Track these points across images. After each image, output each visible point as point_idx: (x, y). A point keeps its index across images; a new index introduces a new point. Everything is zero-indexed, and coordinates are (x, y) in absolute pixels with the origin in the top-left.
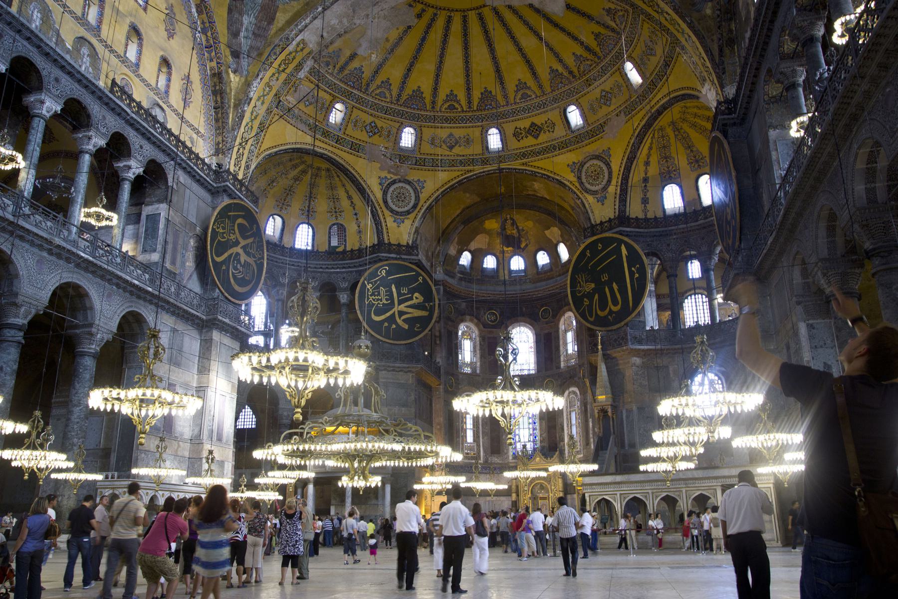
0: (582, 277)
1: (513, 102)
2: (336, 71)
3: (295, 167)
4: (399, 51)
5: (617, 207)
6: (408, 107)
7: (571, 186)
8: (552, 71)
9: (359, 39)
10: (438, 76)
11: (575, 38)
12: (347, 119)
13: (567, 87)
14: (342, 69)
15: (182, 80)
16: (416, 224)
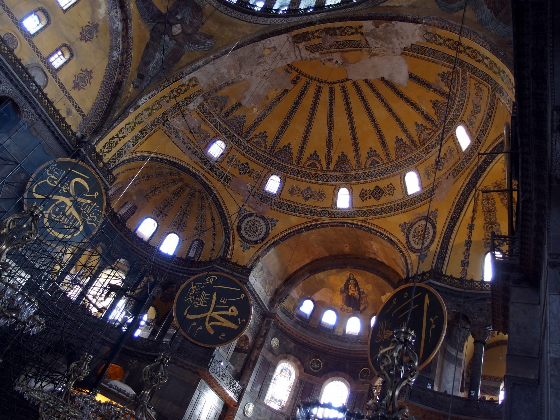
0: (384, 324)
1: (363, 167)
2: (222, 114)
3: (175, 182)
4: (276, 109)
5: (434, 264)
6: (278, 159)
7: (399, 245)
8: (398, 140)
9: (244, 92)
10: (306, 137)
11: (417, 108)
12: (225, 155)
13: (409, 156)
14: (228, 113)
15: (81, 70)
16: (258, 254)
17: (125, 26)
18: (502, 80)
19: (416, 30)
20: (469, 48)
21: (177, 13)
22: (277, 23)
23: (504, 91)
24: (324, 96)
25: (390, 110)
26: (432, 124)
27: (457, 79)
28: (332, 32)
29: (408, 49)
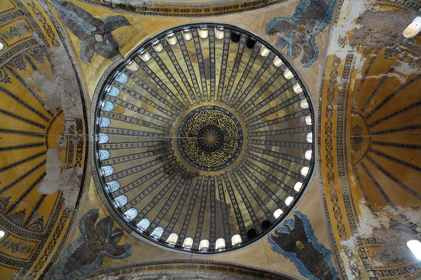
2: (28, 54)
4: (29, 95)
11: (21, 199)
17: (107, 4)
18: (31, 274)
19: (72, 204)
20: (55, 243)
21: (110, 41)
22: (92, 107)
23: (22, 277)
24: (37, 130)
25: (22, 178)
26: (9, 210)
27: (38, 230)
28: (80, 145)
29: (62, 196)
